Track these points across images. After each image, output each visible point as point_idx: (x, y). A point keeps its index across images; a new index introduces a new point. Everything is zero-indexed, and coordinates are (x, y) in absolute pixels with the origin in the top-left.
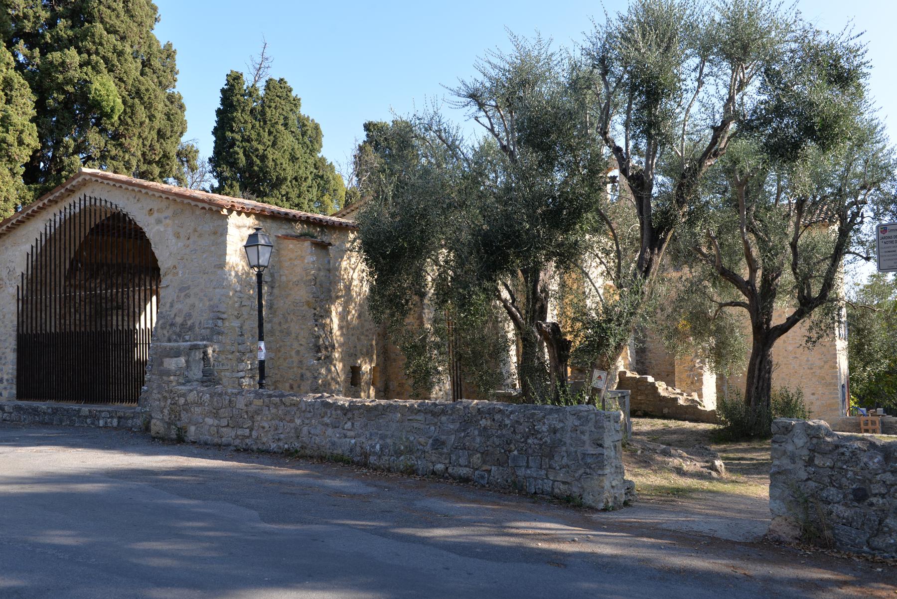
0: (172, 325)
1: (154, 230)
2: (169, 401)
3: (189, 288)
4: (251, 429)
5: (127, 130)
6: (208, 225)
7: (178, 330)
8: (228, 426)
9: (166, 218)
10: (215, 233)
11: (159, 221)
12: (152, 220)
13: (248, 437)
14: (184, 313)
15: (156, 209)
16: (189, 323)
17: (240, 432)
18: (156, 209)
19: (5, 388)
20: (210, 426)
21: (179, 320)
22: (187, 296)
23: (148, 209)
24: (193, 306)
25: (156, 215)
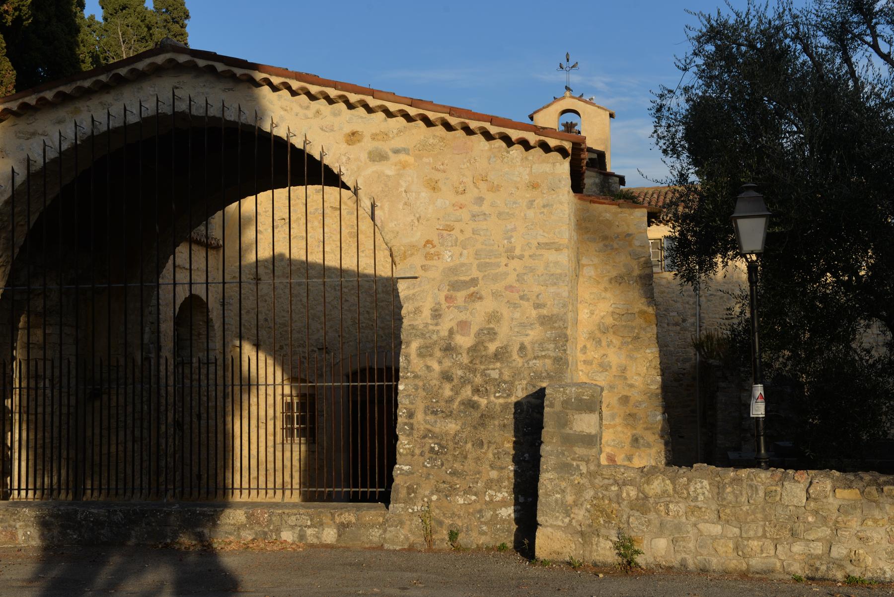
0: (449, 349)
2: (589, 494)
3: (474, 282)
7: (465, 359)
8: (764, 536)
9: (396, 151)
10: (534, 186)
11: (378, 157)
12: (360, 152)
14: (474, 329)
16: (492, 347)
17: (798, 548)
20: (715, 538)
21: (464, 341)
22: (475, 297)
23: (348, 129)
24: (494, 317)
25: (368, 144)
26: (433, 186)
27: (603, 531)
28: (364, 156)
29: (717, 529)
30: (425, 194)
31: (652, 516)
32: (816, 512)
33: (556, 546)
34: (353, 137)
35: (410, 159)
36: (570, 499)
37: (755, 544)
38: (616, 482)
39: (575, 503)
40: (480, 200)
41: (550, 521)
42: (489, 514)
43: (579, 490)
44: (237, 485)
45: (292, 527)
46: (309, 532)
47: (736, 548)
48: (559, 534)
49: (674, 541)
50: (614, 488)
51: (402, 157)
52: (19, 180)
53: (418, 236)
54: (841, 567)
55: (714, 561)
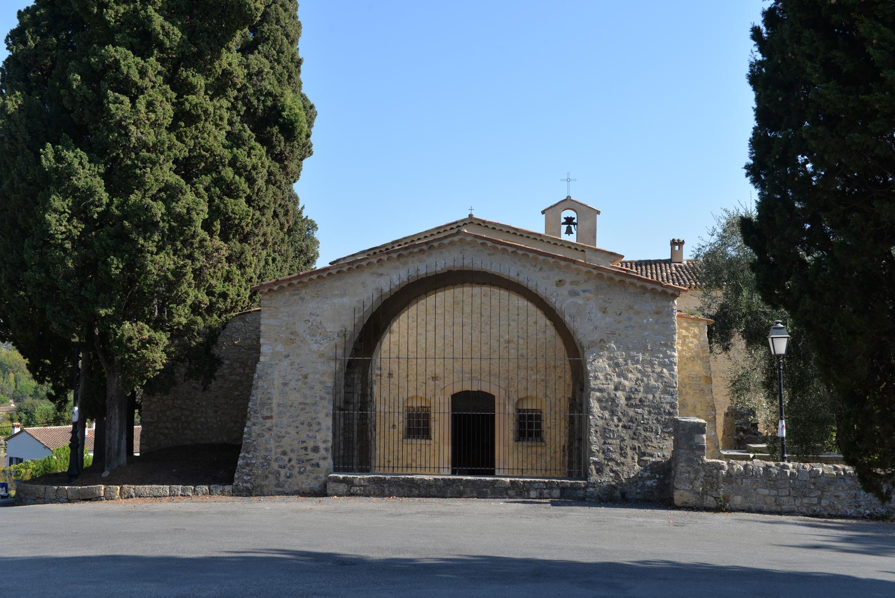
1: (569, 301)
2: (702, 474)
4: (820, 498)
5: (292, 152)
6: (649, 305)
9: (584, 291)
11: (573, 294)
12: (564, 291)
13: (815, 505)
15: (568, 281)
17: (805, 501)
18: (568, 281)
19: (325, 458)
20: (765, 496)
23: (557, 279)
25: (568, 287)
26: (604, 311)
27: (709, 492)
28: (566, 293)
29: (766, 492)
30: (599, 315)
31: (734, 485)
32: (814, 484)
33: (685, 500)
34: (560, 283)
35: (592, 296)
36: (692, 476)
37: (785, 499)
38: (716, 468)
39: (695, 479)
40: (630, 319)
41: (683, 487)
42: (640, 484)
43: (697, 472)
44: (377, 464)
45: (536, 489)
46: (545, 491)
47: (775, 501)
48: (686, 493)
49: (746, 497)
50: (715, 471)
51: (587, 294)
52: (375, 298)
53: (596, 337)
54: (825, 510)
55: (765, 507)
